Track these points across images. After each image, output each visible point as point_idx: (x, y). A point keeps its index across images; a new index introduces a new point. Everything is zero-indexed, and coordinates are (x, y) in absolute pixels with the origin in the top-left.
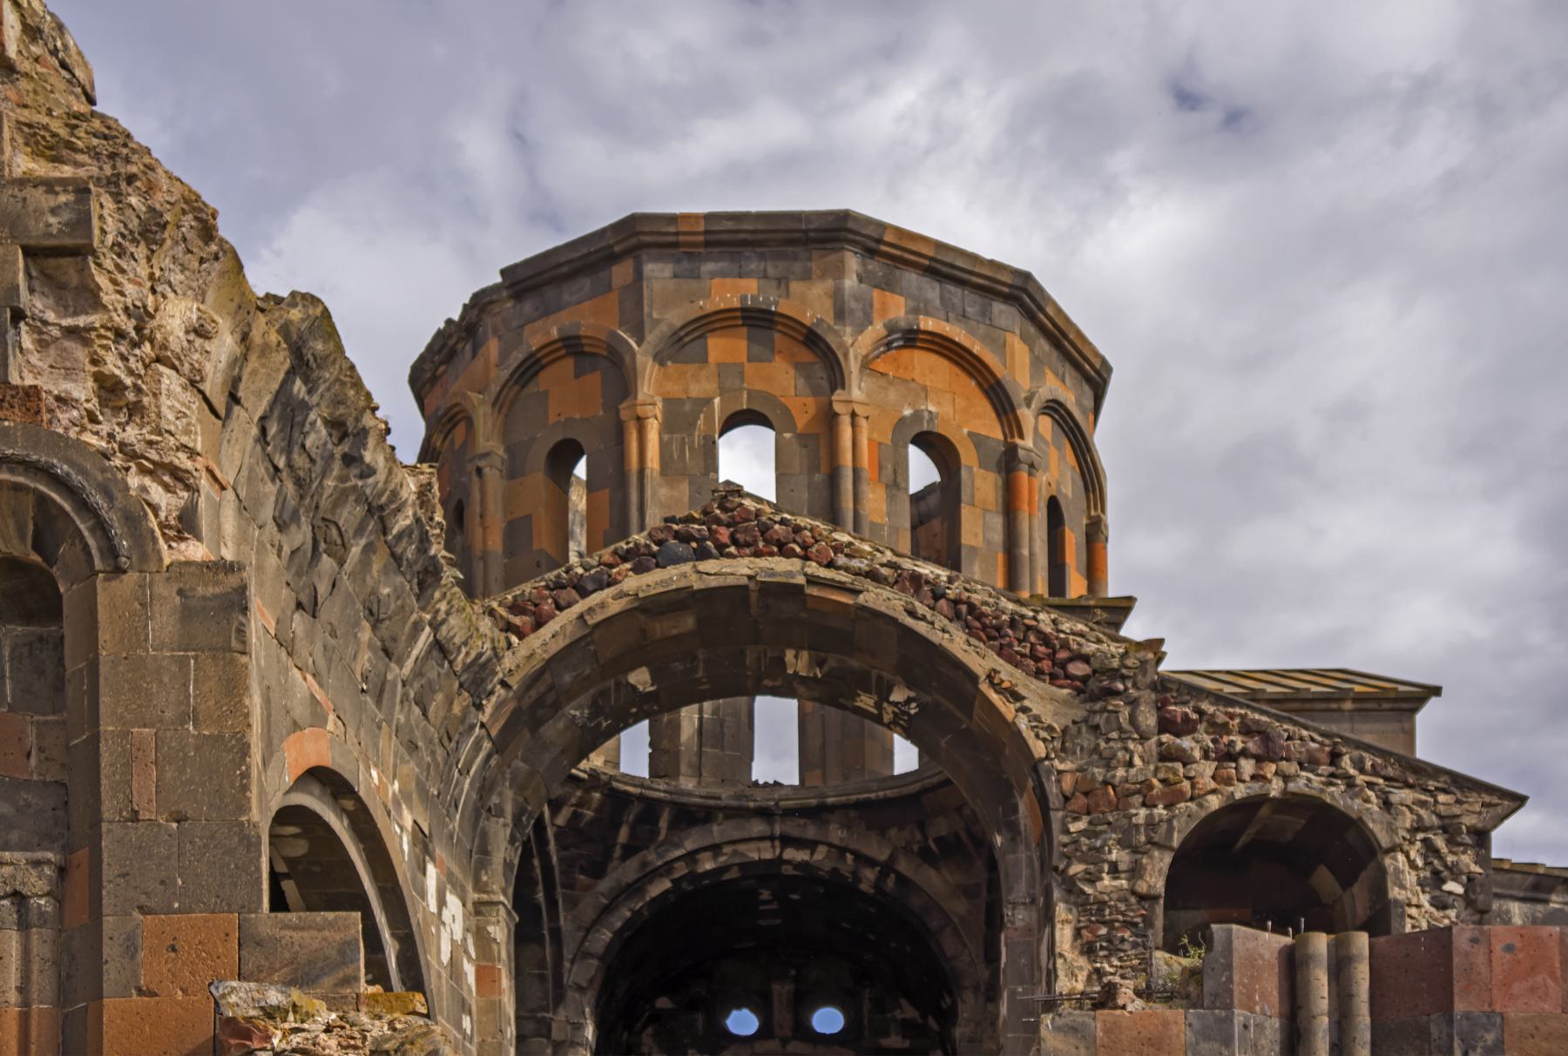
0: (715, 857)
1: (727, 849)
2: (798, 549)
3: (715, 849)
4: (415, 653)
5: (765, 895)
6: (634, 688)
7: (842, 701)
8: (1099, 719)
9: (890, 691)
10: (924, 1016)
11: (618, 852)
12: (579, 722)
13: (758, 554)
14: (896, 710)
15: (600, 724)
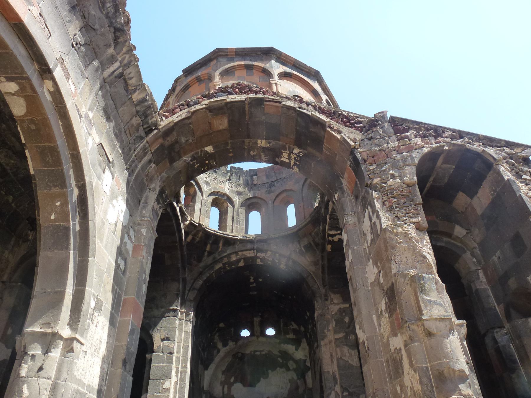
0: (237, 255)
1: (240, 253)
2: (261, 93)
3: (236, 253)
4: (112, 69)
5: (252, 280)
6: (207, 151)
7: (277, 159)
8: (370, 136)
9: (293, 150)
10: (299, 327)
11: (206, 254)
12: (187, 161)
13: (248, 94)
14: (296, 156)
15: (194, 164)
